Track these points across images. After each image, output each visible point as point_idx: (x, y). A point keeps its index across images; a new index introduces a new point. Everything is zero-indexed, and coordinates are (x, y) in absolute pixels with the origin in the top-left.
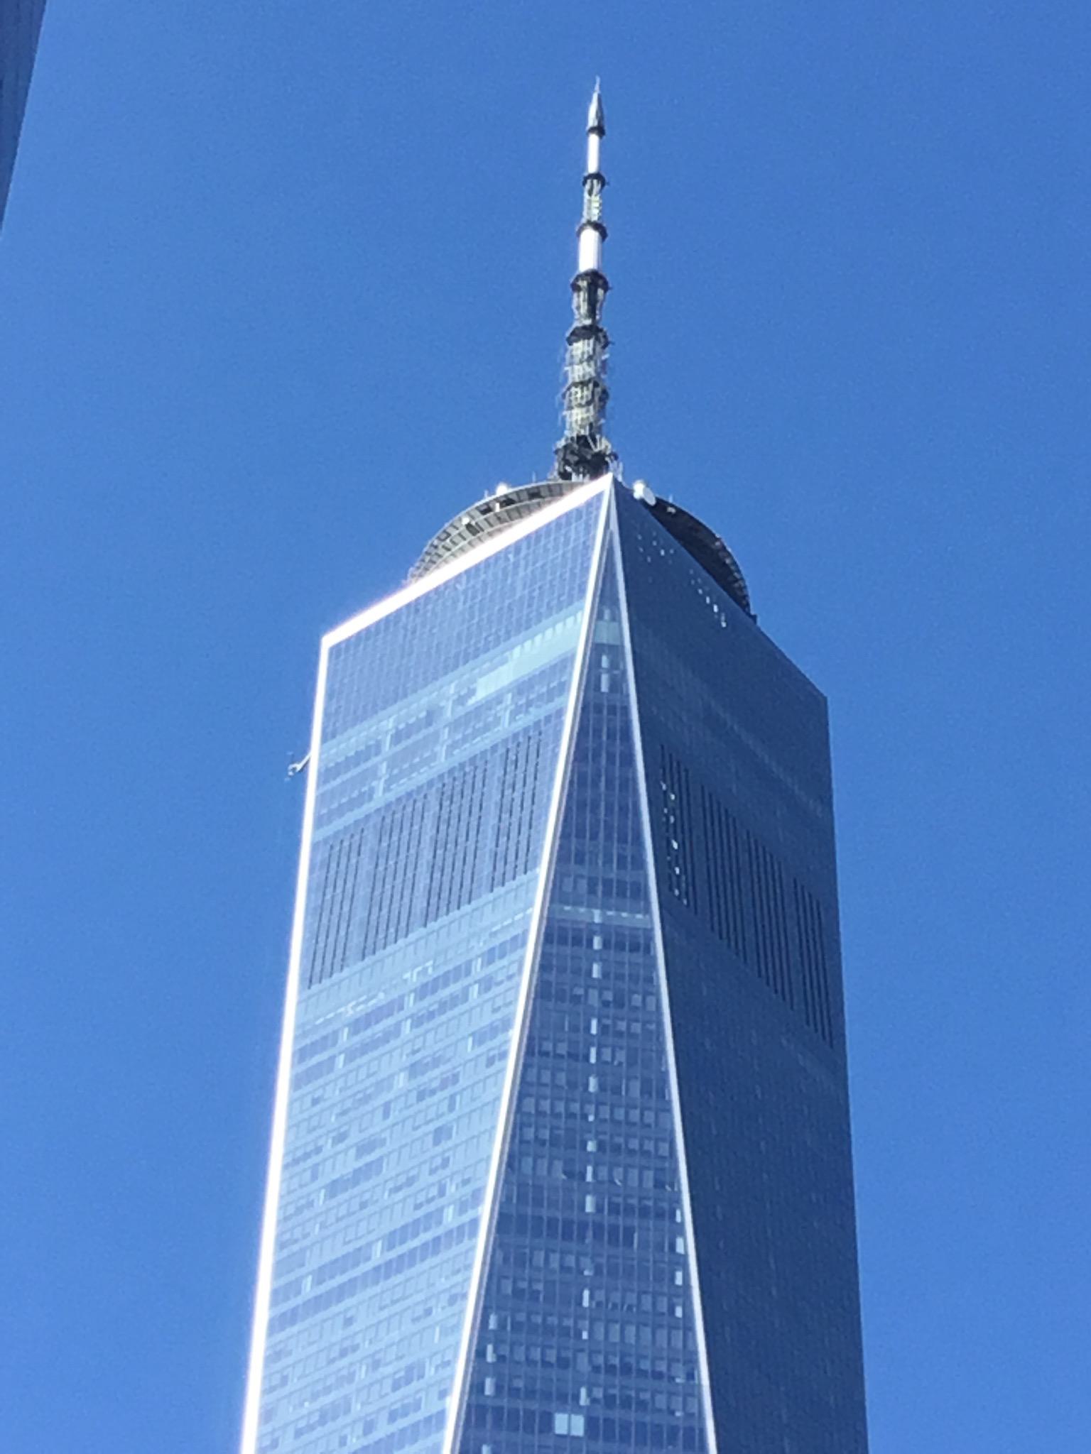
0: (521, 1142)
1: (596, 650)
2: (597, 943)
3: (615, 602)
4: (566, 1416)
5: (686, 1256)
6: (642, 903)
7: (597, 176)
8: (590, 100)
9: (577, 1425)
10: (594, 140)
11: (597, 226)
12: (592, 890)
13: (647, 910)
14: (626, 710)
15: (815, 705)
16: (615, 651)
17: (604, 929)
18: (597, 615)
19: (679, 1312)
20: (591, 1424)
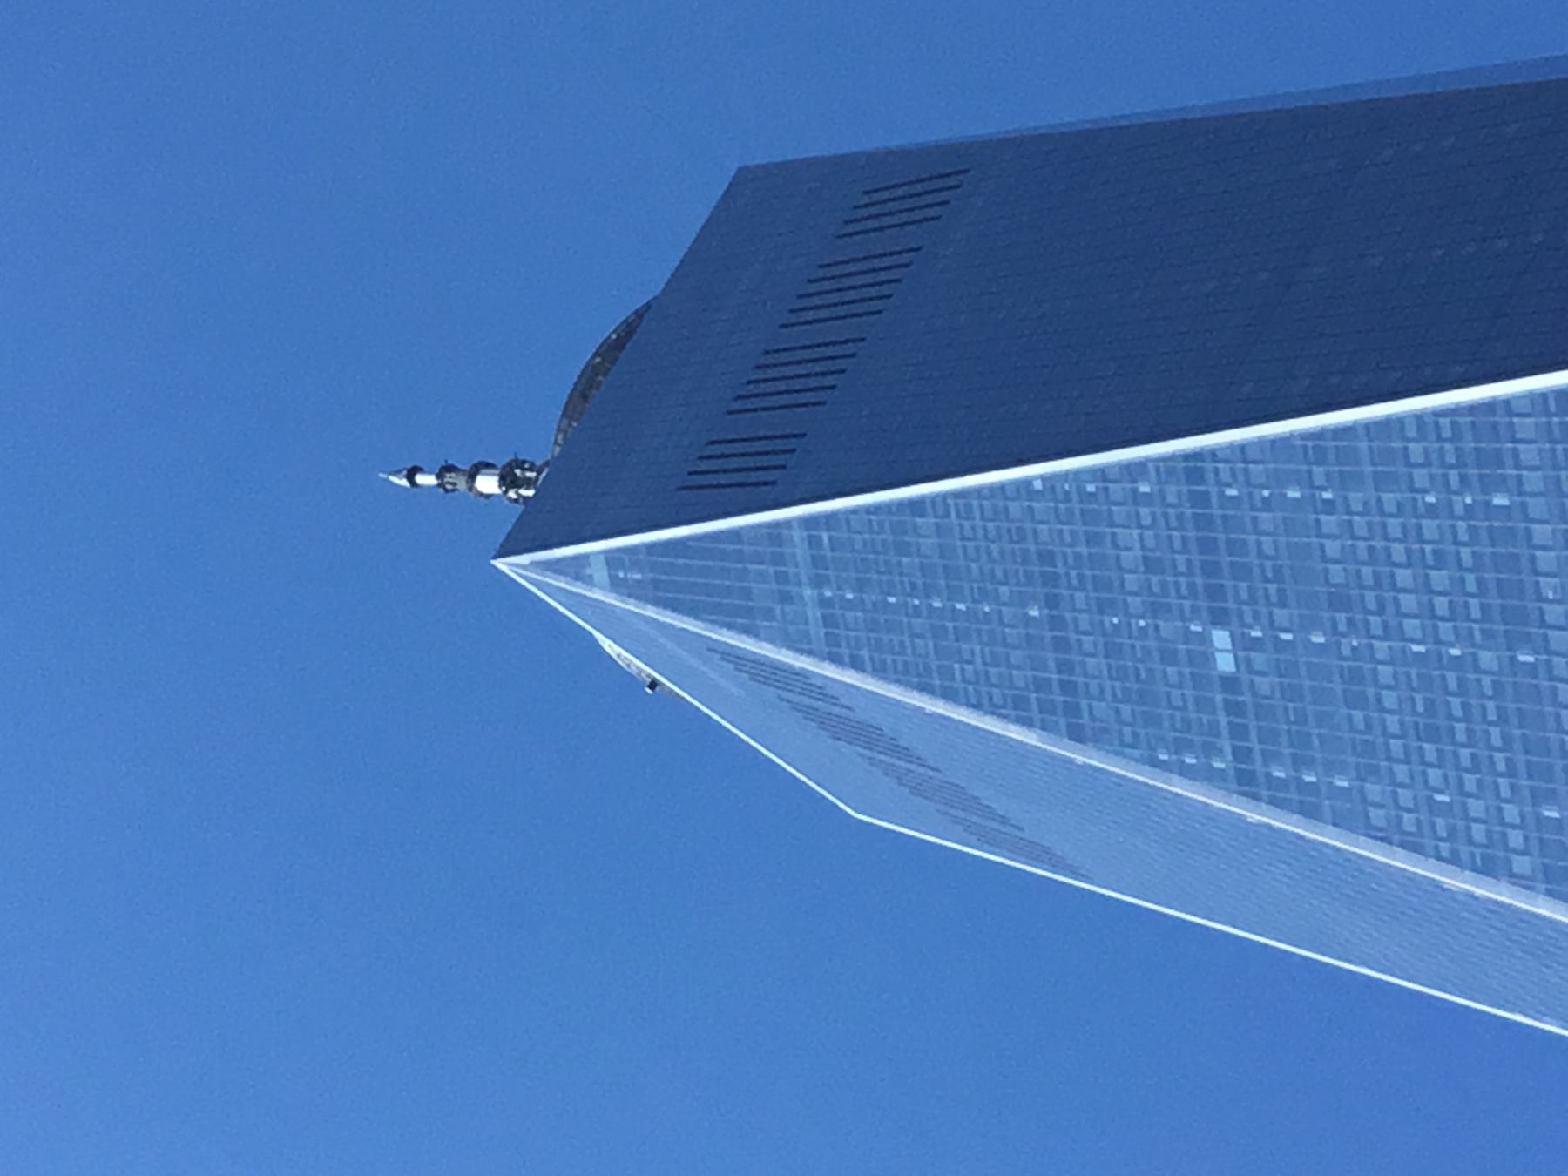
0: (1004, 707)
1: (616, 585)
2: (828, 594)
3: (575, 558)
4: (1218, 655)
5: (1043, 478)
6: (786, 532)
7: (439, 476)
8: (393, 484)
9: (1221, 638)
10: (421, 479)
11: (472, 477)
12: (785, 598)
13: (787, 523)
14: (651, 548)
15: (746, 179)
16: (611, 558)
17: (818, 582)
18: (589, 581)
19: (1091, 488)
20: (1219, 618)
